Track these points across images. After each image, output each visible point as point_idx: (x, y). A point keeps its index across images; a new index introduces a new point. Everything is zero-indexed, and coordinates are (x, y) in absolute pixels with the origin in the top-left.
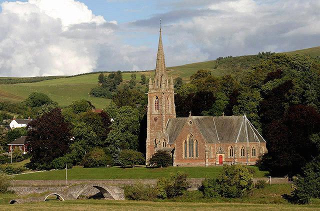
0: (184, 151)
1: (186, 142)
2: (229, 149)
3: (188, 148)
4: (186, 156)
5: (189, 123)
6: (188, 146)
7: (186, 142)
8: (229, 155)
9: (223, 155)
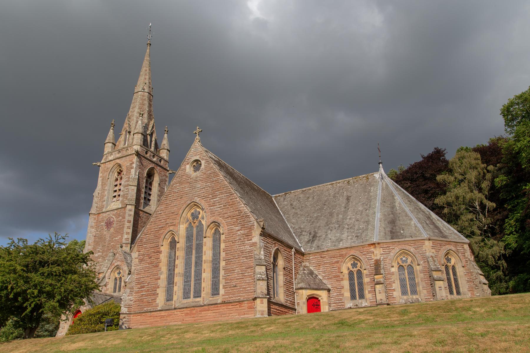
0: (164, 276)
1: (173, 244)
2: (346, 272)
4: (169, 298)
6: (180, 254)
7: (173, 244)
8: (347, 294)
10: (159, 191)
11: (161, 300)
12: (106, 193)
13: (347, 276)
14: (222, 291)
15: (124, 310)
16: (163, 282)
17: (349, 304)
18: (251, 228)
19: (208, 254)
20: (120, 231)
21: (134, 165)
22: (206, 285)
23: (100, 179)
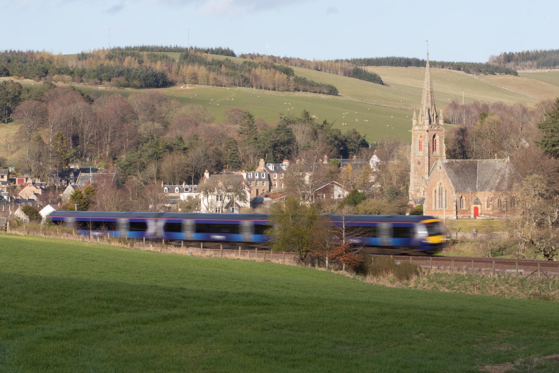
0: (434, 201)
1: (435, 191)
2: (486, 200)
3: (437, 198)
5: (438, 168)
6: (437, 195)
7: (435, 191)
8: (486, 206)
9: (479, 206)
10: (440, 143)
11: (433, 208)
12: (416, 147)
13: (486, 201)
14: (447, 207)
15: (424, 210)
16: (434, 202)
17: (486, 209)
18: (453, 191)
19: (444, 197)
20: (423, 167)
21: (426, 136)
22: (444, 205)
23: (412, 139)
